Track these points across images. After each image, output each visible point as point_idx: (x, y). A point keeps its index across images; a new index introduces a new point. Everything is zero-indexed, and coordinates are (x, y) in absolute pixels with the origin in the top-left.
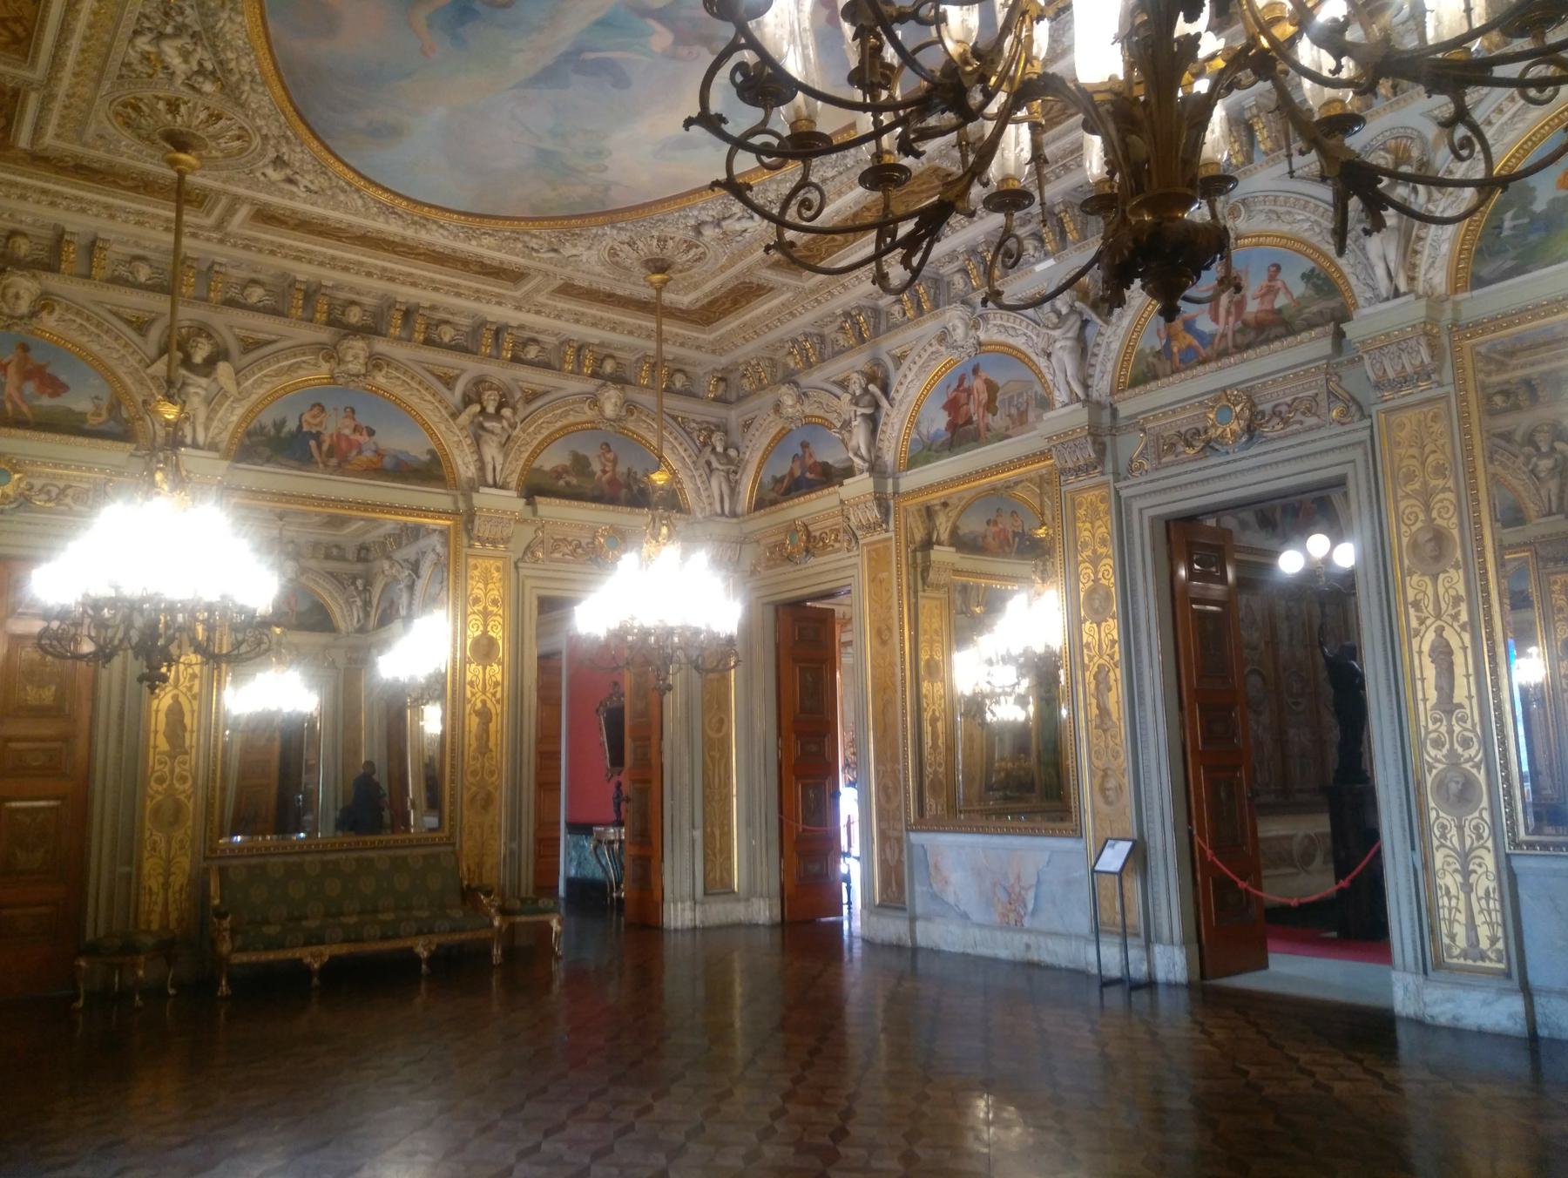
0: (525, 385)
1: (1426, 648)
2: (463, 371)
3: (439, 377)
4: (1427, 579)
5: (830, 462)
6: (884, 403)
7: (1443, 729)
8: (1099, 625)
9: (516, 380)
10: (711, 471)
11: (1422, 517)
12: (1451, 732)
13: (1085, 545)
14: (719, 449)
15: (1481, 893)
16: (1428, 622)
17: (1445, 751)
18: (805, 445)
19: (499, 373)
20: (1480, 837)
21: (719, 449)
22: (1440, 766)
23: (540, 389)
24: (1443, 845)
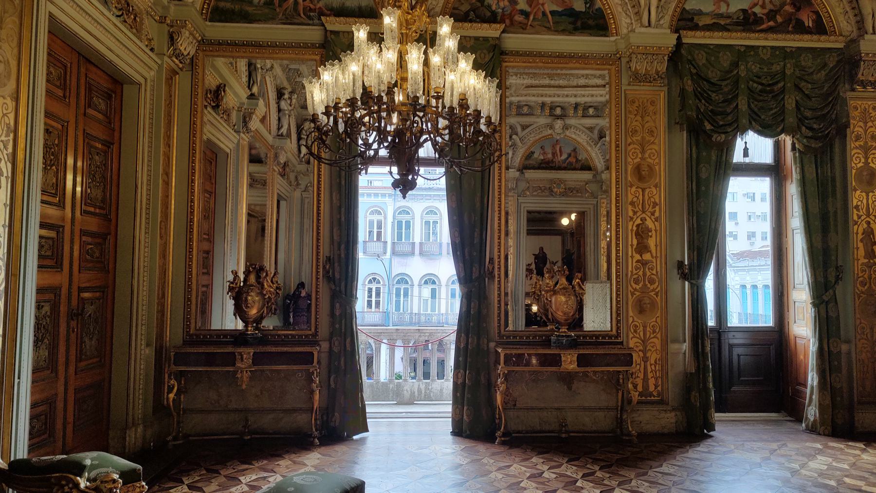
1: (861, 230)
4: (864, 194)
7: (641, 273)
8: (643, 190)
11: (863, 160)
12: (644, 274)
13: (635, 132)
15: (653, 362)
16: (863, 218)
17: (640, 285)
20: (654, 332)
22: (638, 294)
24: (635, 337)
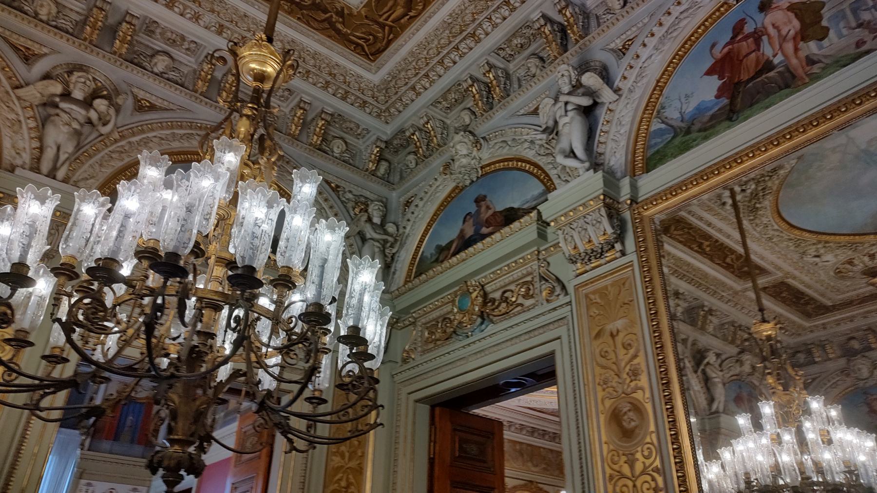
0: (141, 94)
2: (54, 51)
3: (15, 48)
5: (516, 206)
6: (607, 95)
9: (130, 85)
10: (364, 240)
14: (377, 220)
18: (479, 200)
19: (106, 68)
21: (377, 220)
23: (158, 103)
